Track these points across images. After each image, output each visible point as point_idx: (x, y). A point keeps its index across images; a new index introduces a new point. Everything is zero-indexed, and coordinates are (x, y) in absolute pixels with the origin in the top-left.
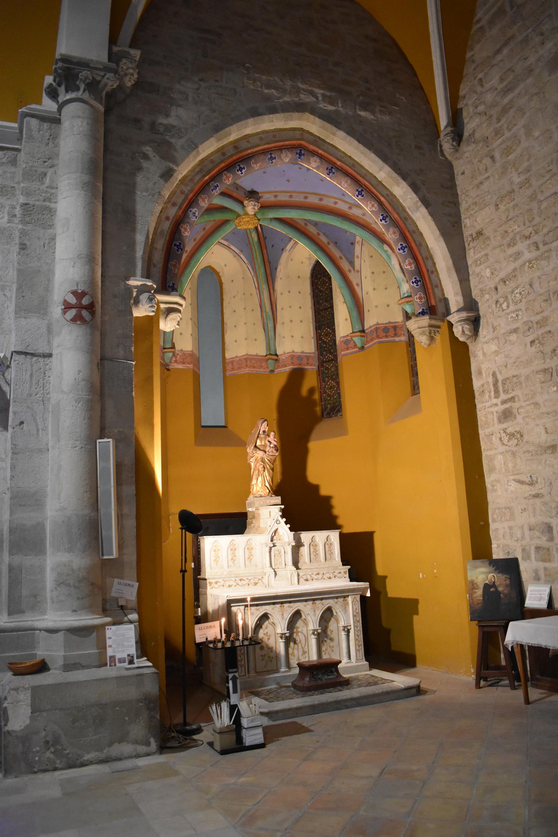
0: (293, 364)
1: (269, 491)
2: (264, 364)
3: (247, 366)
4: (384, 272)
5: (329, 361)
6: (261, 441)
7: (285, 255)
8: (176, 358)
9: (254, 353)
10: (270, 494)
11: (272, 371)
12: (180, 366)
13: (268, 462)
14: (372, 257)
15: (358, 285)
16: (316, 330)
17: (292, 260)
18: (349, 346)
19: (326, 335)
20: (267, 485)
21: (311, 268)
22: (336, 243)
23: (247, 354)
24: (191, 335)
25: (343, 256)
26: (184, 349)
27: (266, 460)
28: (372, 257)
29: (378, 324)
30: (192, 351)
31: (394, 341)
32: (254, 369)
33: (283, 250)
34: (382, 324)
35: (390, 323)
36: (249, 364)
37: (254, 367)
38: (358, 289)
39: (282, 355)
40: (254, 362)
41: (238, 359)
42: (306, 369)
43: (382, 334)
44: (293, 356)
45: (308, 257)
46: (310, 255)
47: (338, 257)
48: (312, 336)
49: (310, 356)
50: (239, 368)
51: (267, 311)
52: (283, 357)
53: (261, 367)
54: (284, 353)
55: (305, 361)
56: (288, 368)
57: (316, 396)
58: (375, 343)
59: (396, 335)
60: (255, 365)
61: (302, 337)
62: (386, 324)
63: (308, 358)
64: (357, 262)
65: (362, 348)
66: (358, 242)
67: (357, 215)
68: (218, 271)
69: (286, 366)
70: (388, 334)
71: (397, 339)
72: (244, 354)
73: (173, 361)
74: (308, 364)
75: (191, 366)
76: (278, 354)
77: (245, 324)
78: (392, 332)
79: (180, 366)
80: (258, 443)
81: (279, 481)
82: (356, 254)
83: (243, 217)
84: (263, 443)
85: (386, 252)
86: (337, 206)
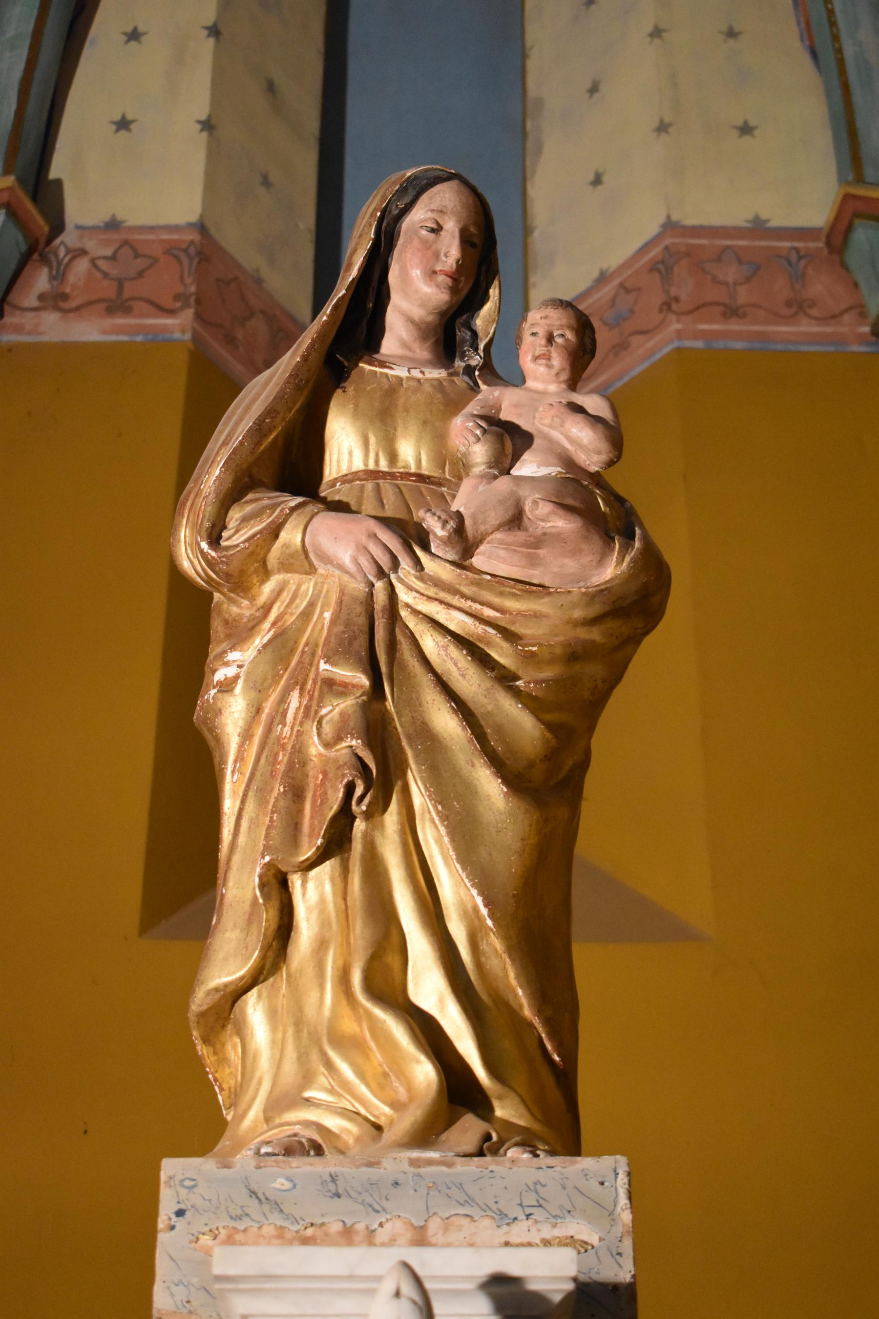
1: (459, 1093)
2: (821, 286)
3: (667, 306)
6: (383, 416)
8: (59, 275)
10: (469, 1129)
12: (89, 331)
13: (469, 681)
20: (429, 988)
23: (670, 226)
24: (208, 125)
26: (134, 218)
27: (430, 643)
30: (201, 227)
32: (734, 326)
37: (732, 312)
40: (731, 273)
41: (608, 290)
53: (799, 307)
60: (743, 296)
72: (652, 229)
73: (31, 301)
75: (179, 326)
77: (657, 33)
79: (89, 331)
80: (346, 446)
84: (411, 452)
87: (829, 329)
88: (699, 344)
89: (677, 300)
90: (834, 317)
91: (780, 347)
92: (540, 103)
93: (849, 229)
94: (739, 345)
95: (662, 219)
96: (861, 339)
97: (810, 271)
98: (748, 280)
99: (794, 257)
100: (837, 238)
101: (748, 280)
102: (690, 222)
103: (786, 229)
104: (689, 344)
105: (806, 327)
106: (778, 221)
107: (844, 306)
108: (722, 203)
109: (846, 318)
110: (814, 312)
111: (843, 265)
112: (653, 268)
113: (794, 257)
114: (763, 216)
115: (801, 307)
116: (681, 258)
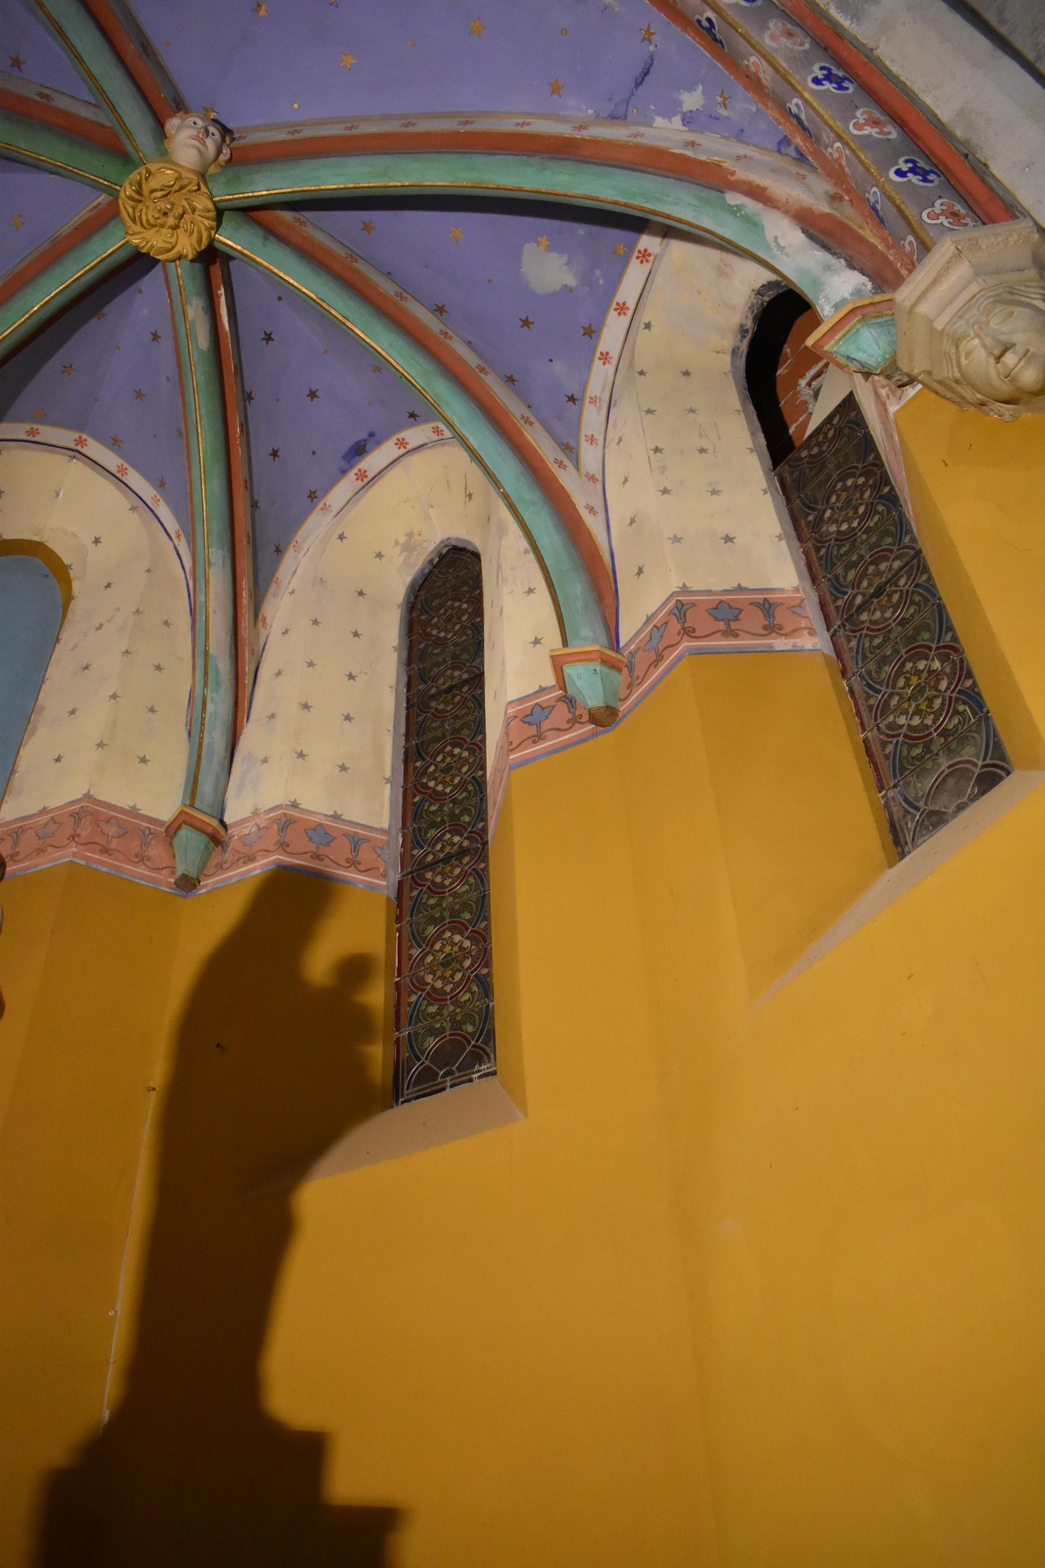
0: (283, 846)
2: (156, 851)
3: (73, 837)
4: (703, 451)
5: (447, 860)
7: (316, 527)
9: (125, 803)
11: (188, 884)
14: (649, 411)
15: (591, 510)
16: (406, 762)
17: (341, 537)
18: (546, 725)
19: (446, 770)
21: (409, 579)
22: (511, 380)
23: (88, 797)
25: (532, 419)
28: (649, 411)
29: (685, 590)
31: (770, 651)
32: (104, 858)
33: (313, 496)
34: (709, 592)
35: (740, 589)
36: (85, 831)
37: (105, 851)
38: (594, 524)
39: (244, 821)
41: (45, 818)
42: (344, 881)
43: (703, 623)
44: (287, 821)
45: (402, 539)
46: (410, 535)
47: (518, 416)
48: (388, 774)
49: (367, 840)
50: (41, 851)
51: (212, 650)
52: (250, 828)
53: (141, 859)
54: (256, 813)
55: (341, 850)
56: (258, 868)
57: (376, 996)
58: (679, 658)
59: (772, 629)
61: (343, 768)
62: (726, 592)
63: (357, 842)
64: (589, 456)
65: (605, 718)
66: (593, 401)
67: (608, 137)
68: (67, 561)
69: (252, 859)
70: (734, 625)
71: (780, 644)
74: (353, 863)
76: (228, 819)
77: (114, 696)
78: (754, 620)
81: (106, 1415)
82: (586, 430)
83: (153, 167)
85: (735, 211)
86: (526, 129)
87: (154, 875)
88: (83, 863)
89: (79, 836)
90: (158, 869)
91: (125, 876)
92: (43, 708)
93: (179, 827)
94: (104, 869)
95: (85, 792)
96: (168, 885)
97: (153, 842)
98: (119, 837)
99: (147, 832)
100: (172, 830)
101: (119, 837)
102: (98, 798)
103: (148, 817)
104: (77, 860)
105: (142, 870)
106: (144, 811)
107: (164, 865)
108: (118, 794)
109: (164, 872)
110: (148, 863)
111: (171, 844)
112: (72, 815)
113: (147, 832)
114: (138, 807)
115: (143, 859)
116: (88, 817)
